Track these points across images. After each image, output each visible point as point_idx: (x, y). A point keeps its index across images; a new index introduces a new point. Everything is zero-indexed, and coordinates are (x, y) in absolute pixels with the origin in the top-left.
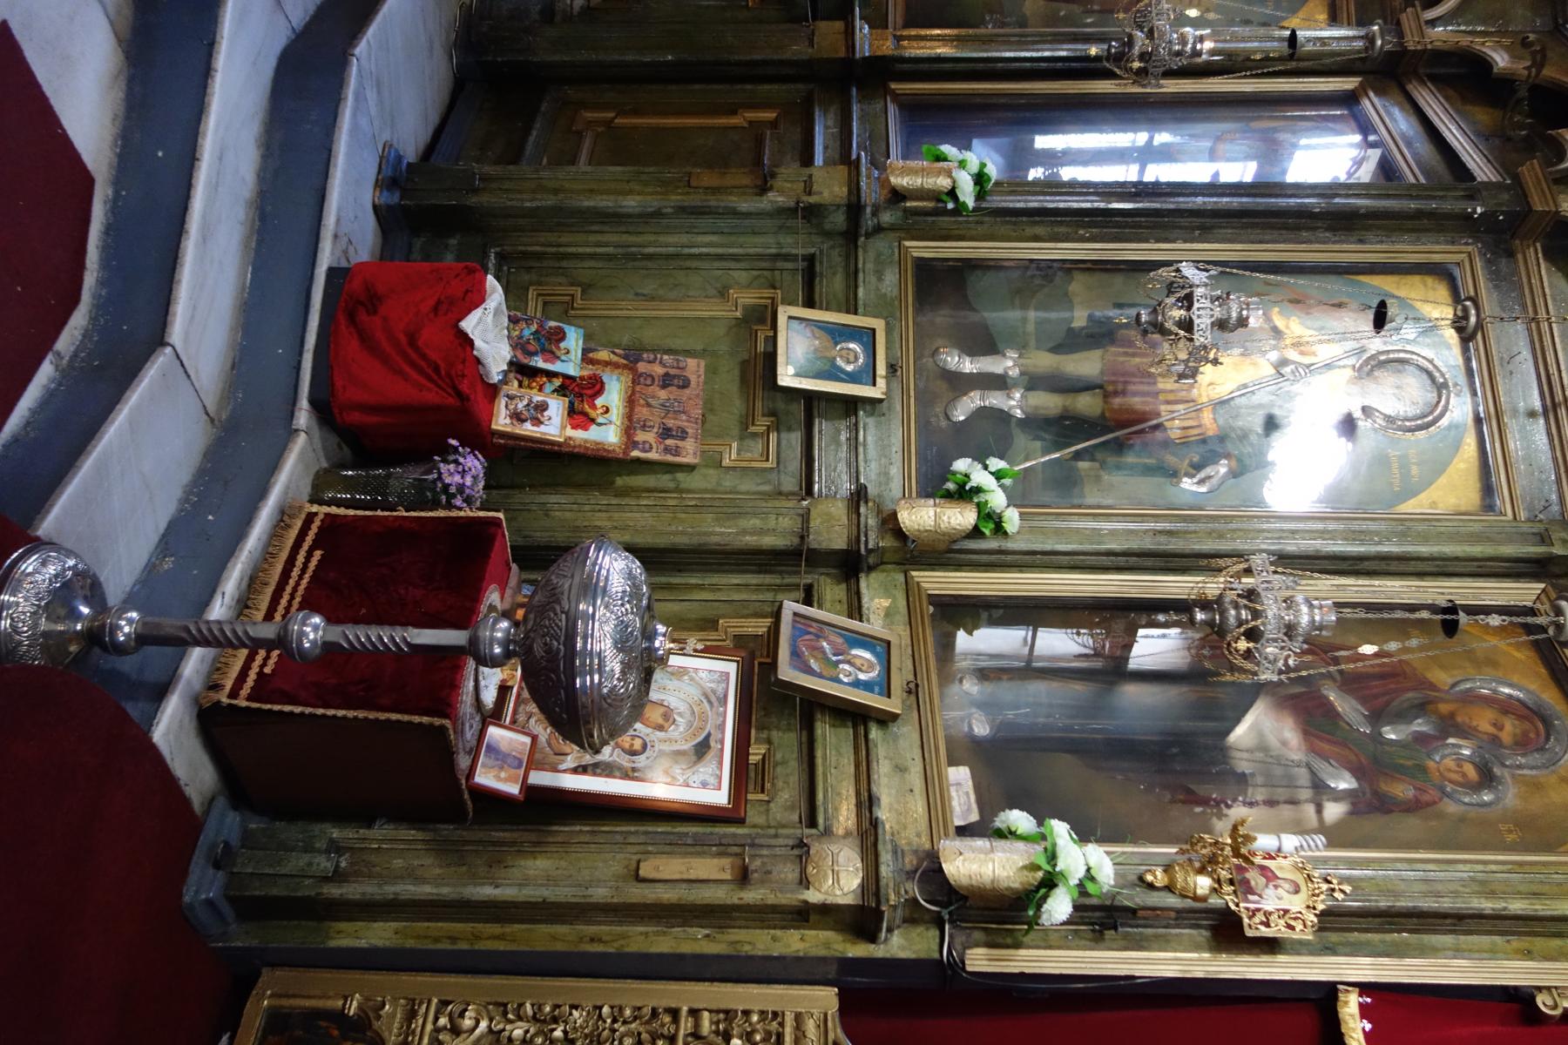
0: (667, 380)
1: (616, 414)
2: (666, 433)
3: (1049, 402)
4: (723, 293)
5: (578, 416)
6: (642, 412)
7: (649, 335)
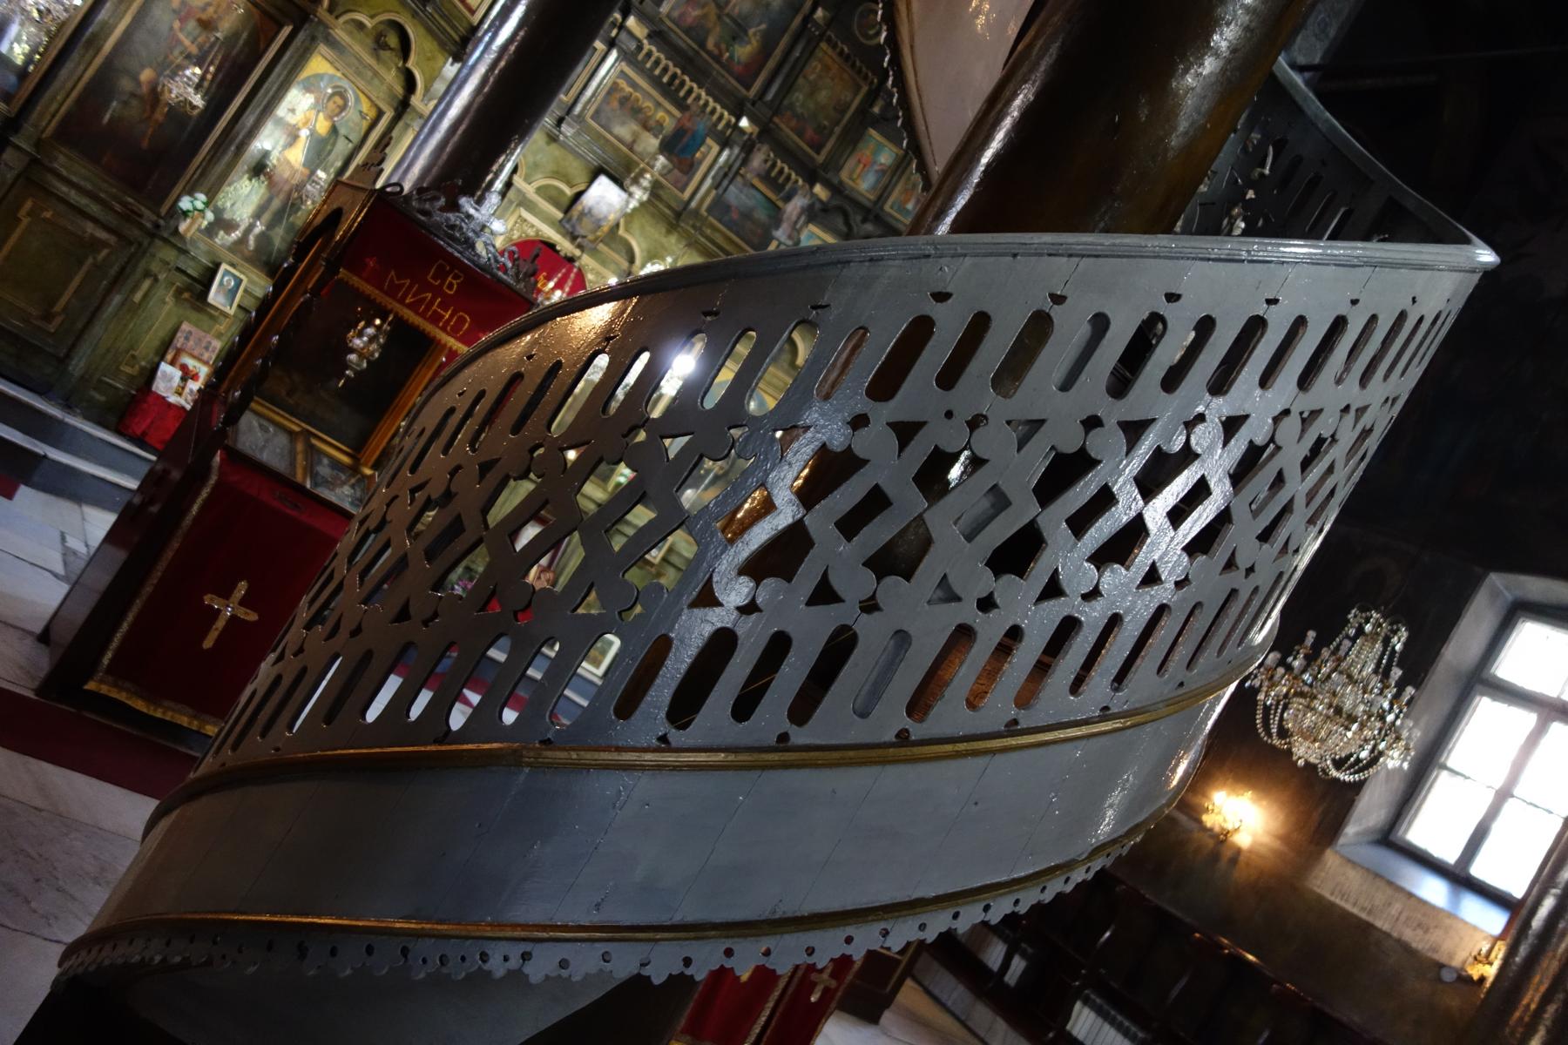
0: (187, 339)
1: (198, 364)
2: (207, 348)
3: (267, 216)
4: (164, 303)
5: (195, 377)
6: (196, 353)
7: (163, 334)
